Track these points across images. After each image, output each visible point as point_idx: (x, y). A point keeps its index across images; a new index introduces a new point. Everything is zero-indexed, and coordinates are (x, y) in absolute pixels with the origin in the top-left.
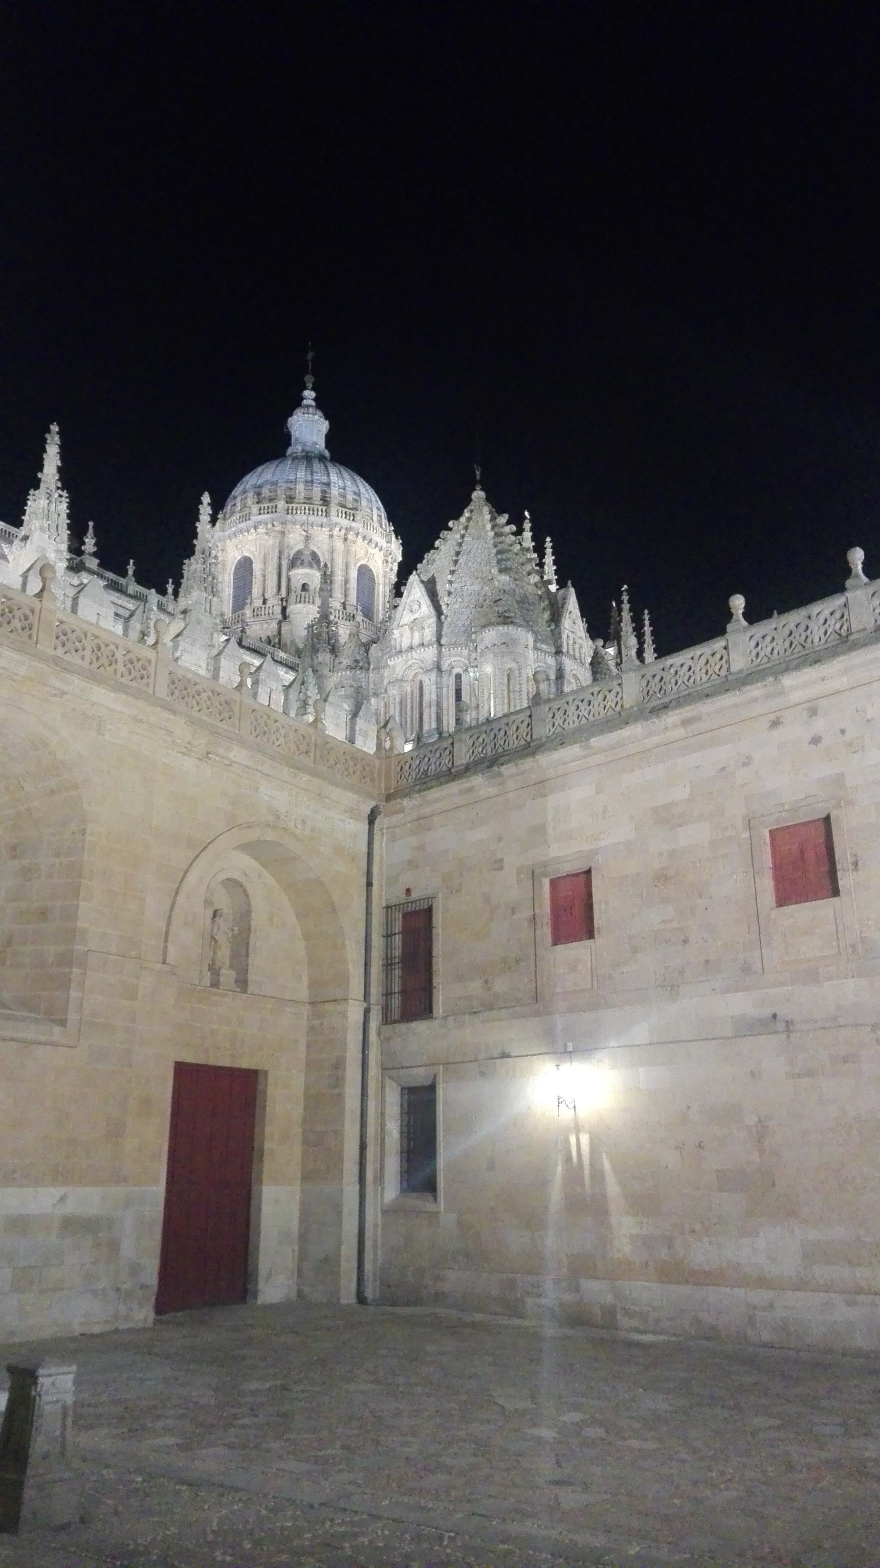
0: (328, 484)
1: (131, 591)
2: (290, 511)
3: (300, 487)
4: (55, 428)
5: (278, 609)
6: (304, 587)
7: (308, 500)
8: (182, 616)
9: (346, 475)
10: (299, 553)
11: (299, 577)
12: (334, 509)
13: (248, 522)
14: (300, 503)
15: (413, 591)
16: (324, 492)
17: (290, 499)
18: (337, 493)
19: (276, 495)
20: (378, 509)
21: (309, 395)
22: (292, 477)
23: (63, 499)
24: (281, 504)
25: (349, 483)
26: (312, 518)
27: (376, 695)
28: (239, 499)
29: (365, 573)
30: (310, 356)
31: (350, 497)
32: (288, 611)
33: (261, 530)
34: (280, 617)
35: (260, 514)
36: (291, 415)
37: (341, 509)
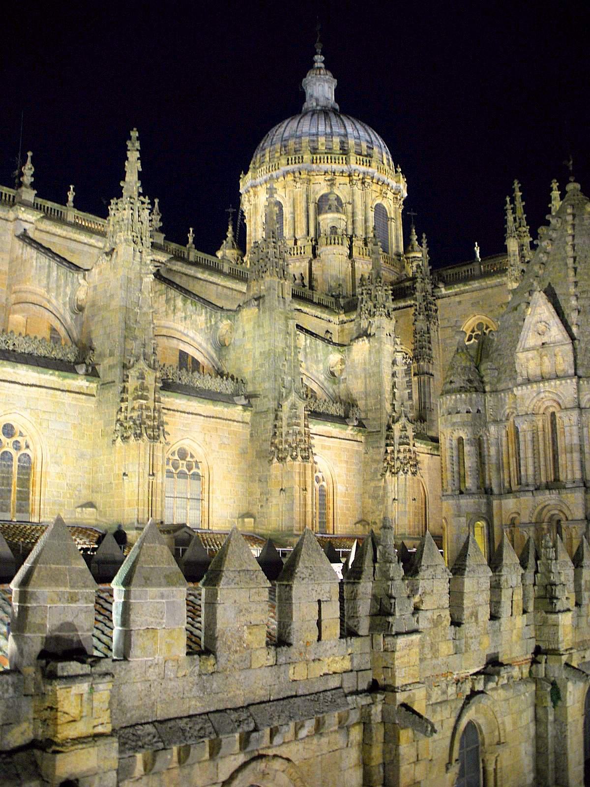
0: (346, 135)
1: (192, 258)
2: (315, 161)
3: (322, 140)
4: (134, 134)
5: (309, 250)
6: (334, 229)
7: (330, 150)
8: (256, 303)
9: (358, 126)
10: (324, 198)
11: (329, 221)
12: (353, 159)
13: (277, 171)
14: (322, 153)
15: (538, 310)
16: (342, 143)
17: (314, 151)
18: (354, 142)
19: (301, 147)
20: (387, 153)
21: (319, 59)
22: (314, 131)
23: (146, 206)
24: (307, 157)
25: (362, 133)
26: (335, 166)
27: (496, 422)
28: (267, 151)
29: (380, 210)
30: (319, 27)
31: (364, 145)
32: (318, 252)
33: (290, 178)
34: (311, 256)
35: (288, 164)
36: (305, 76)
37: (358, 157)
